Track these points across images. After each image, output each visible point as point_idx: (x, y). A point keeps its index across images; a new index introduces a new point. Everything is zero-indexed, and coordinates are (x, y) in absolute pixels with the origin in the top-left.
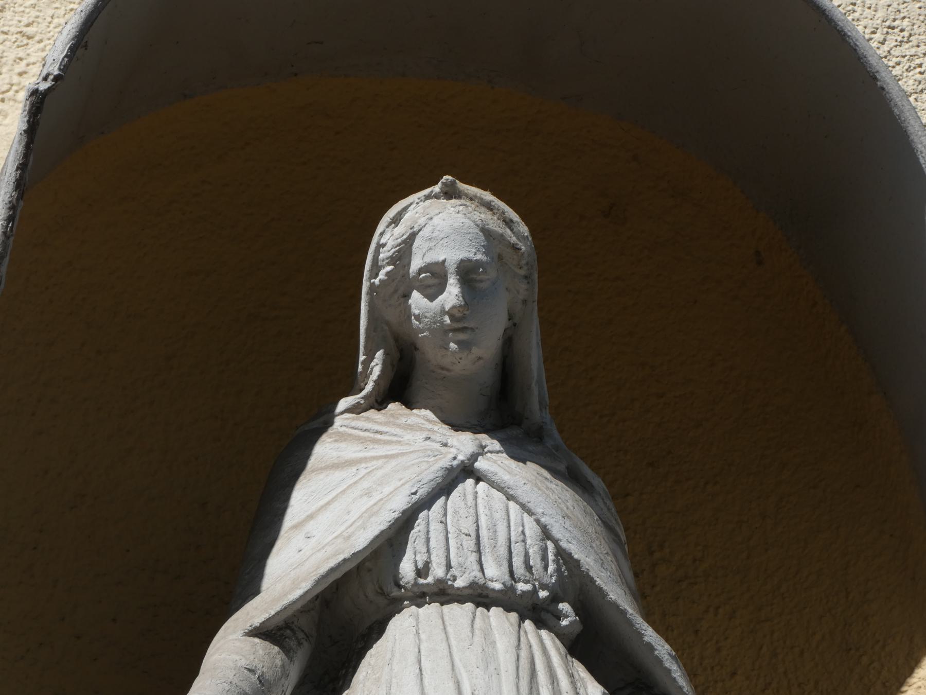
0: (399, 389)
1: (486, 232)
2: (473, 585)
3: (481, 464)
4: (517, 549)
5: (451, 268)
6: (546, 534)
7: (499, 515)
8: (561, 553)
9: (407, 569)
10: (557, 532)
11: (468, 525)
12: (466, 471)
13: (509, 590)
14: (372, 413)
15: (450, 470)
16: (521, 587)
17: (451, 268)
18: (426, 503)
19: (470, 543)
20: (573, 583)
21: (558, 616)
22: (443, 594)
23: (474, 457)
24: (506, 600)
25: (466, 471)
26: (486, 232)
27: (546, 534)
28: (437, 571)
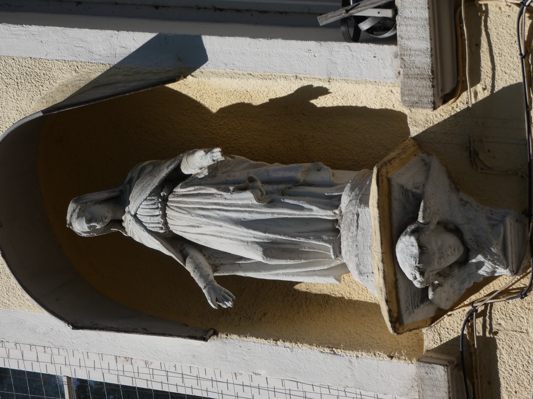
0: (119, 222)
1: (78, 217)
2: (162, 218)
3: (133, 213)
4: (151, 207)
5: (89, 225)
6: (146, 199)
7: (144, 210)
8: (149, 196)
9: (162, 231)
10: (145, 197)
11: (148, 218)
12: (135, 216)
13: (161, 209)
14: (127, 230)
15: (136, 221)
16: (160, 206)
17: (89, 225)
18: (145, 228)
19: (152, 218)
20: (156, 192)
21: (164, 195)
22: (166, 223)
23: (131, 215)
24: (164, 209)
25: (135, 216)
26: (78, 217)
27: (146, 199)
28: (161, 226)
